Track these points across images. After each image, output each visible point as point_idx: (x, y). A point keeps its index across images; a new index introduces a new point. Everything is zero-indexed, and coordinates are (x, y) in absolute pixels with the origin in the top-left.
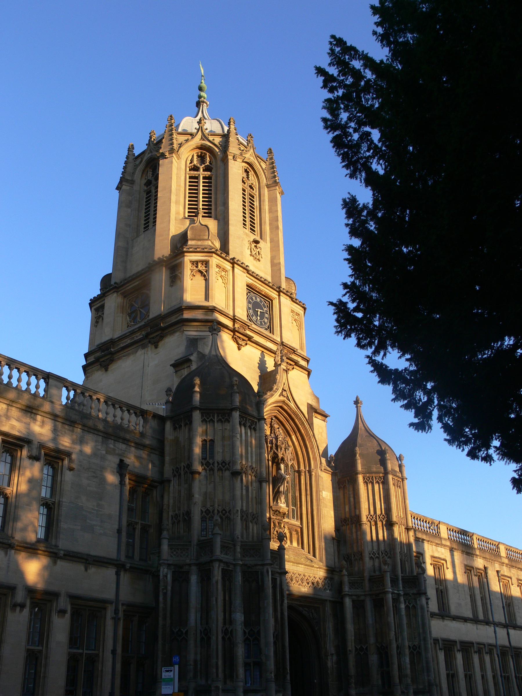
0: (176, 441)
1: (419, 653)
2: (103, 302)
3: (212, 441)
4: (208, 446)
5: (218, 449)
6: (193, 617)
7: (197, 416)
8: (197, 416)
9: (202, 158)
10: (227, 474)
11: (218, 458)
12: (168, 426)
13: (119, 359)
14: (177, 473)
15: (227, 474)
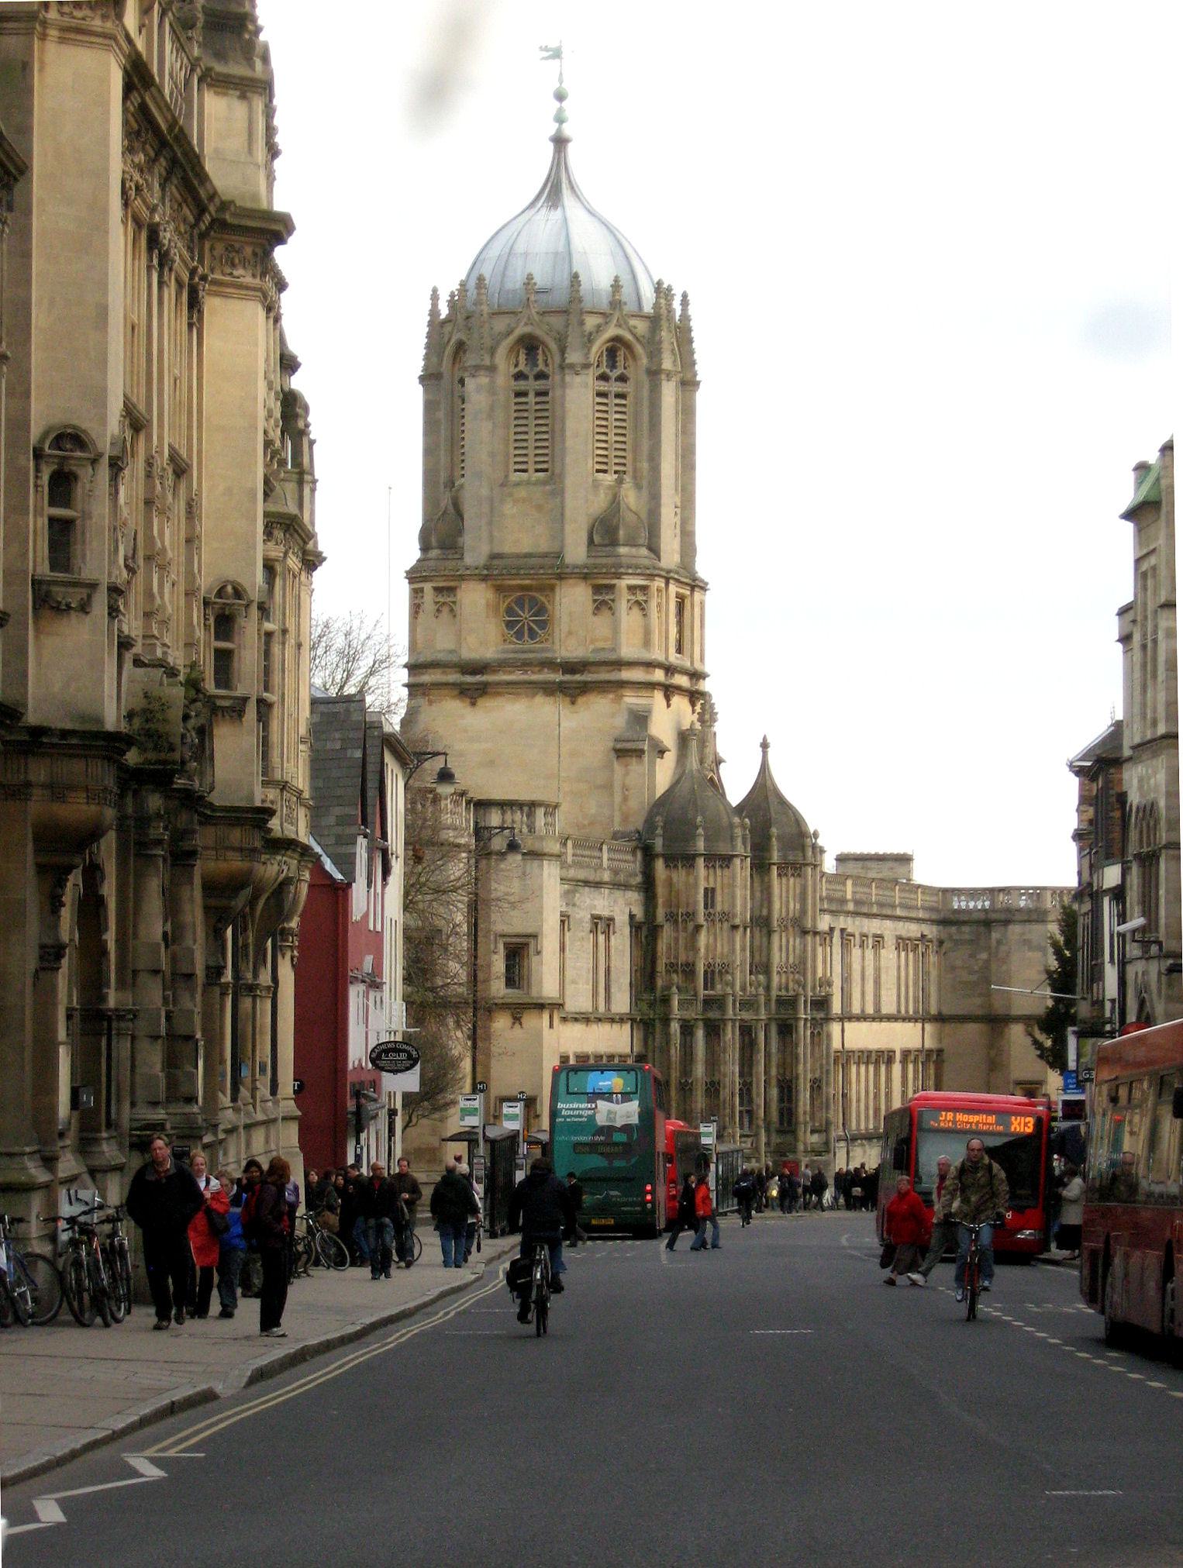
0: (670, 883)
1: (819, 1087)
2: (452, 584)
3: (713, 890)
4: (710, 893)
5: (719, 898)
6: (699, 1070)
7: (701, 862)
8: (701, 862)
9: (612, 353)
10: (726, 925)
11: (719, 908)
12: (660, 864)
13: (499, 694)
14: (671, 917)
15: (726, 925)
